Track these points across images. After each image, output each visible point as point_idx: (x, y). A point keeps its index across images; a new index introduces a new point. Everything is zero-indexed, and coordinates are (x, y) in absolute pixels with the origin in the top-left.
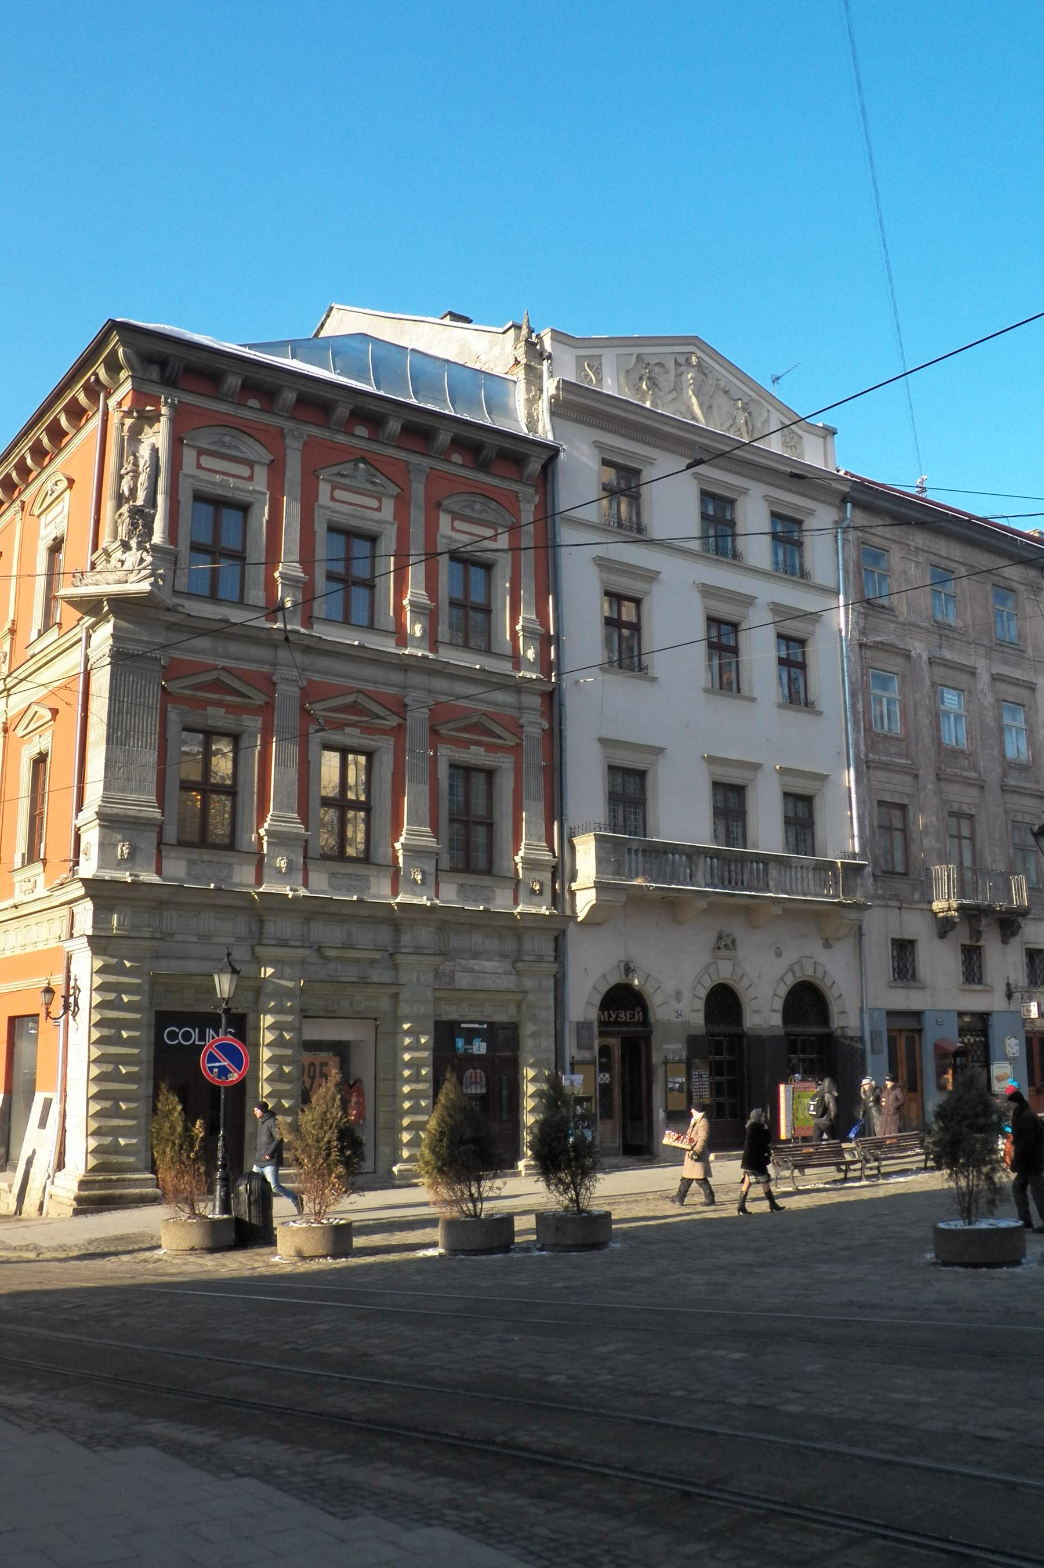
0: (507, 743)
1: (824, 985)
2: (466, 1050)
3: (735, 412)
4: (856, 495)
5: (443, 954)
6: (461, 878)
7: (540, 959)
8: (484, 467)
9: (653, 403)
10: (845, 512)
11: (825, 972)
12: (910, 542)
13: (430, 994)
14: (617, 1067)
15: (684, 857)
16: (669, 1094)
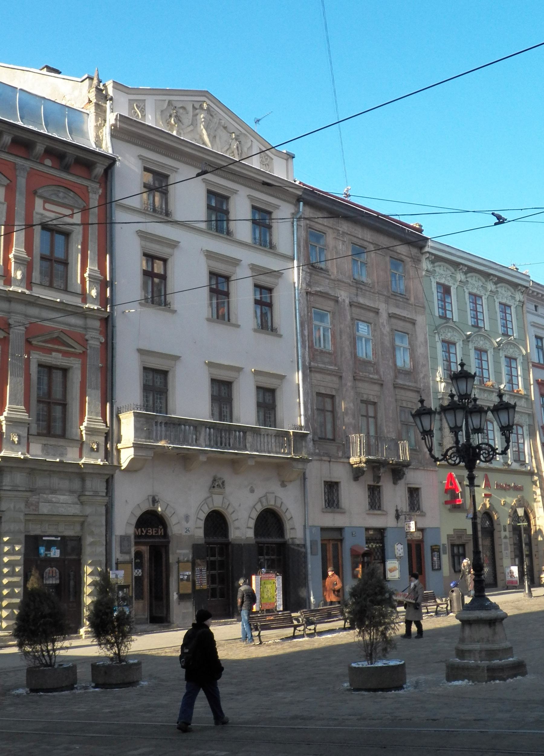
0: (77, 351)
1: (281, 511)
2: (46, 554)
3: (230, 141)
4: (305, 197)
5: (31, 491)
6: (45, 440)
7: (96, 494)
8: (66, 169)
9: (178, 132)
10: (299, 208)
11: (282, 503)
12: (339, 229)
13: (22, 517)
14: (146, 565)
15: (192, 428)
16: (181, 583)
